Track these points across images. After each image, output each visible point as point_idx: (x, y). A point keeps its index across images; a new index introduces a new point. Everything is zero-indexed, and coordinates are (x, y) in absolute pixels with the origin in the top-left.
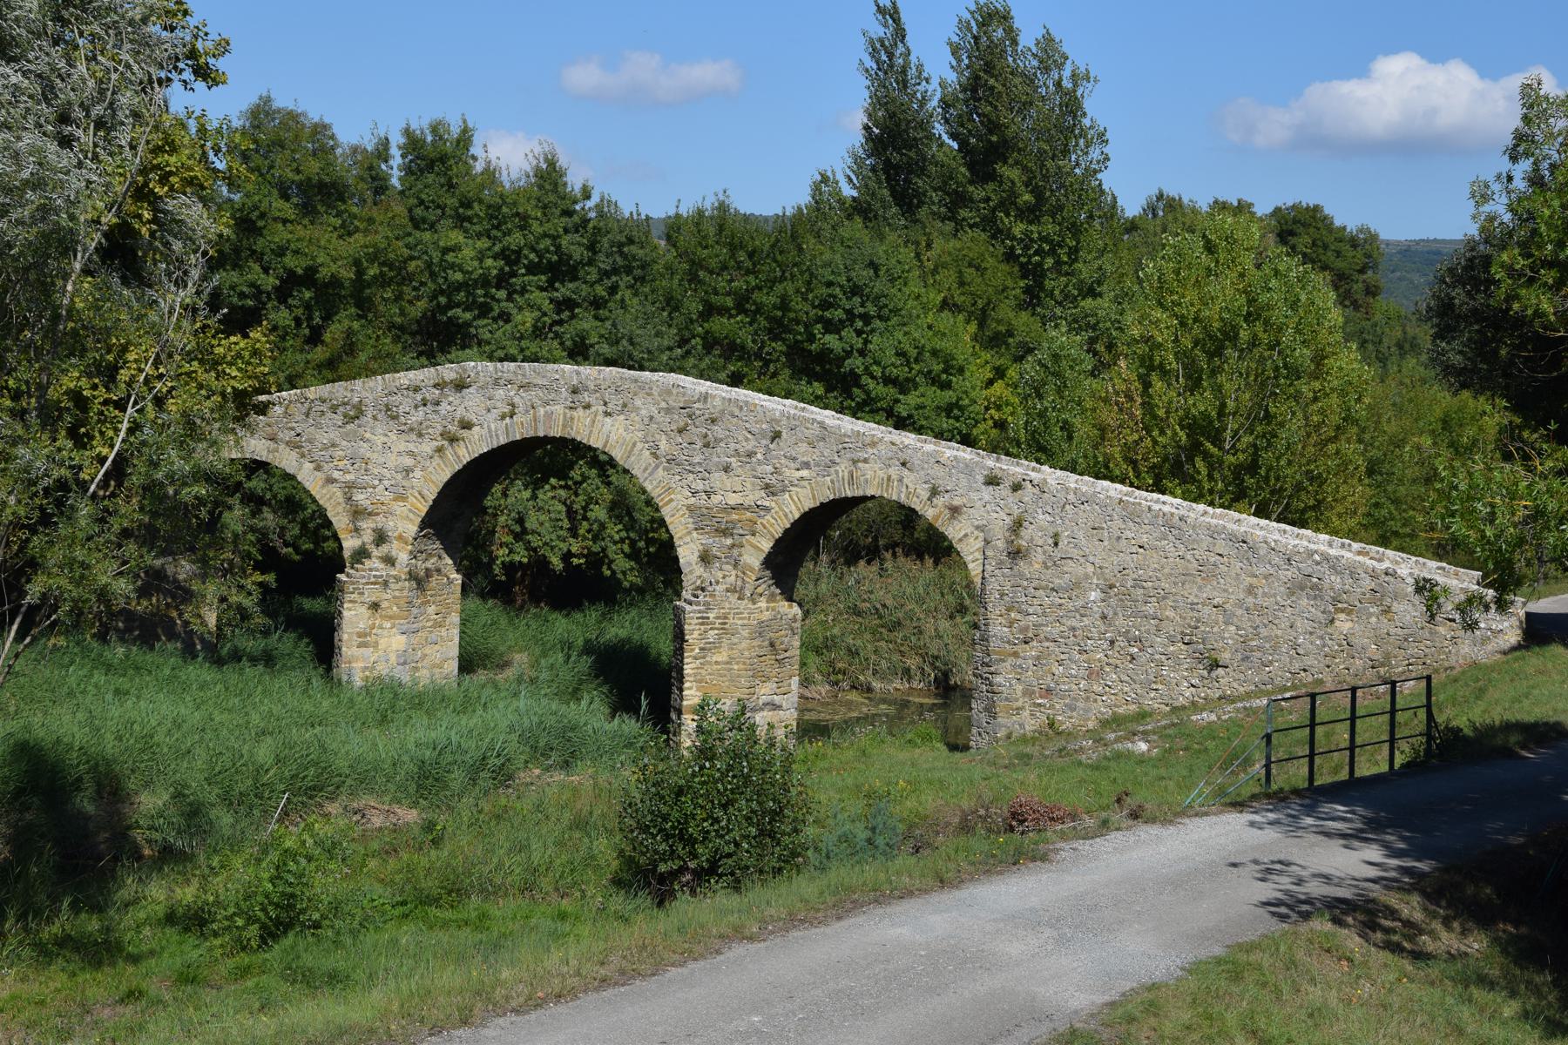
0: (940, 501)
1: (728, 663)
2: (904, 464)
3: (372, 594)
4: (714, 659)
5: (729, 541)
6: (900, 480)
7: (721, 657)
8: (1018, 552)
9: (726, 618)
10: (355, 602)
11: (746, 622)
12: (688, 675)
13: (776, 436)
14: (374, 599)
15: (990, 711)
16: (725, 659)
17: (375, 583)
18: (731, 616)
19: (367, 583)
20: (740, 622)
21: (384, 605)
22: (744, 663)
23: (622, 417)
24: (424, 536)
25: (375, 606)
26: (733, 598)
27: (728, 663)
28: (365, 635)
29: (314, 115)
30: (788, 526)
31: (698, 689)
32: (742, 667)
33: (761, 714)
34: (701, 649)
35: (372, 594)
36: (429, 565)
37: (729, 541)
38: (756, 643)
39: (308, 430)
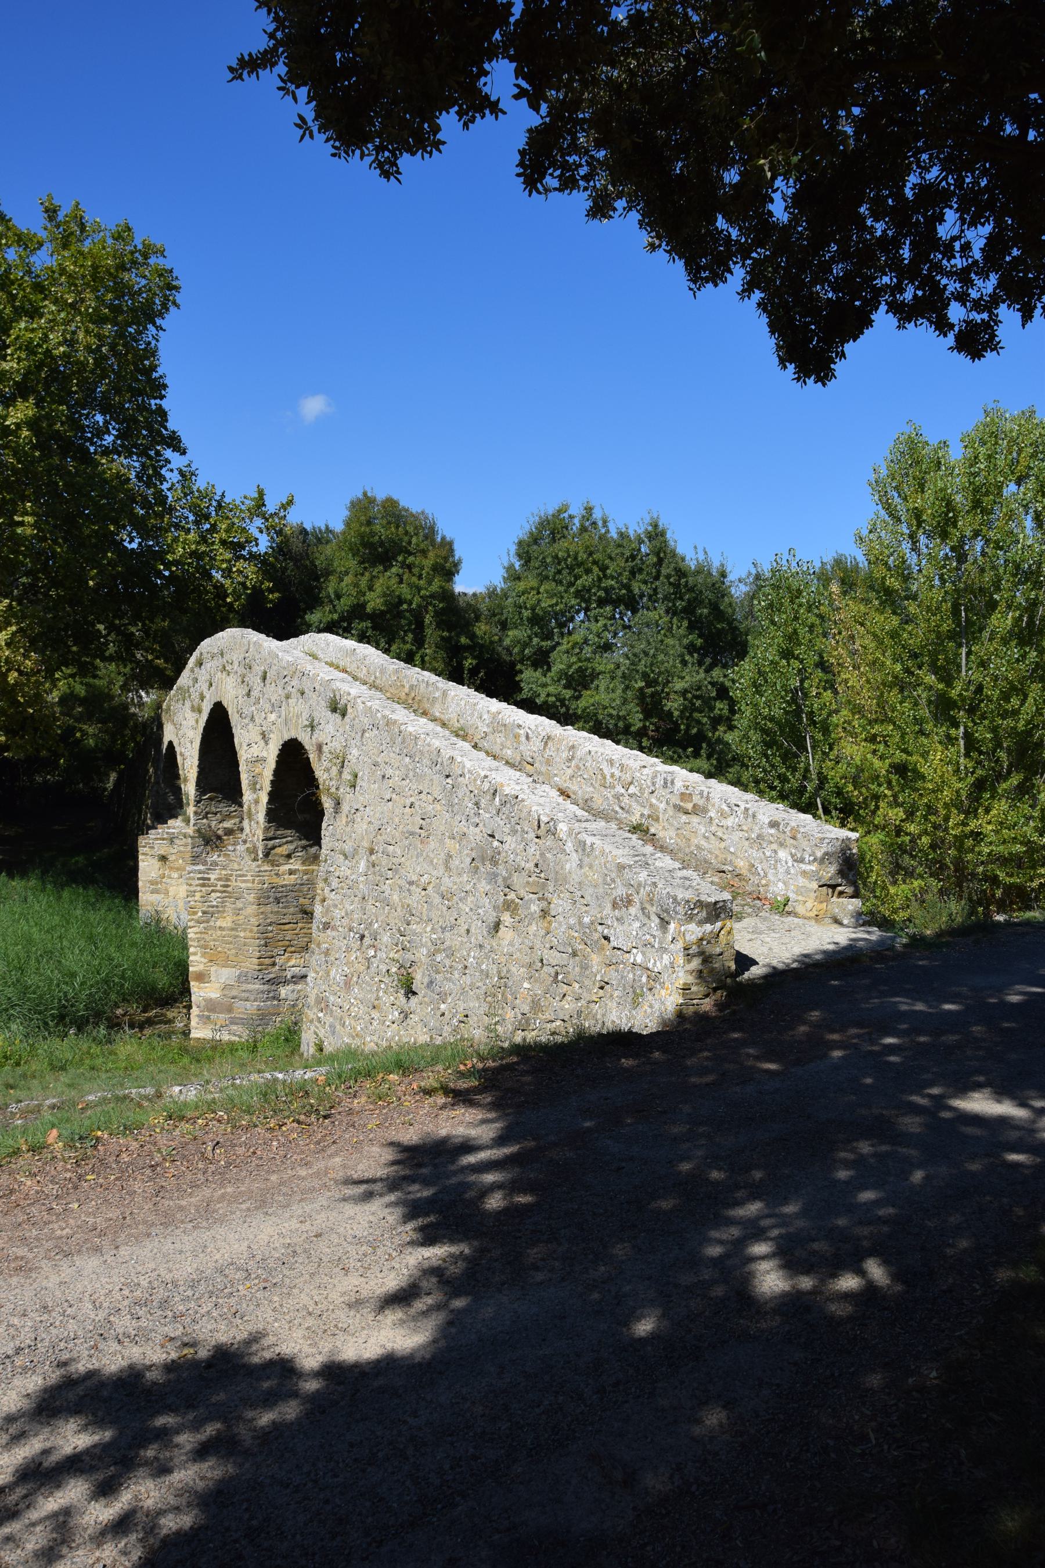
1: (232, 929)
3: (161, 848)
4: (218, 924)
7: (226, 922)
9: (228, 880)
10: (146, 854)
11: (250, 885)
12: (193, 940)
14: (162, 852)
16: (230, 925)
17: (163, 839)
18: (233, 878)
19: (157, 839)
20: (243, 885)
21: (172, 858)
22: (251, 931)
24: (211, 799)
25: (163, 858)
26: (248, 859)
27: (232, 929)
28: (157, 883)
29: (380, 495)
30: (271, 778)
31: (204, 955)
32: (249, 934)
33: (290, 987)
34: (204, 913)
35: (161, 848)
36: (227, 824)
38: (268, 908)
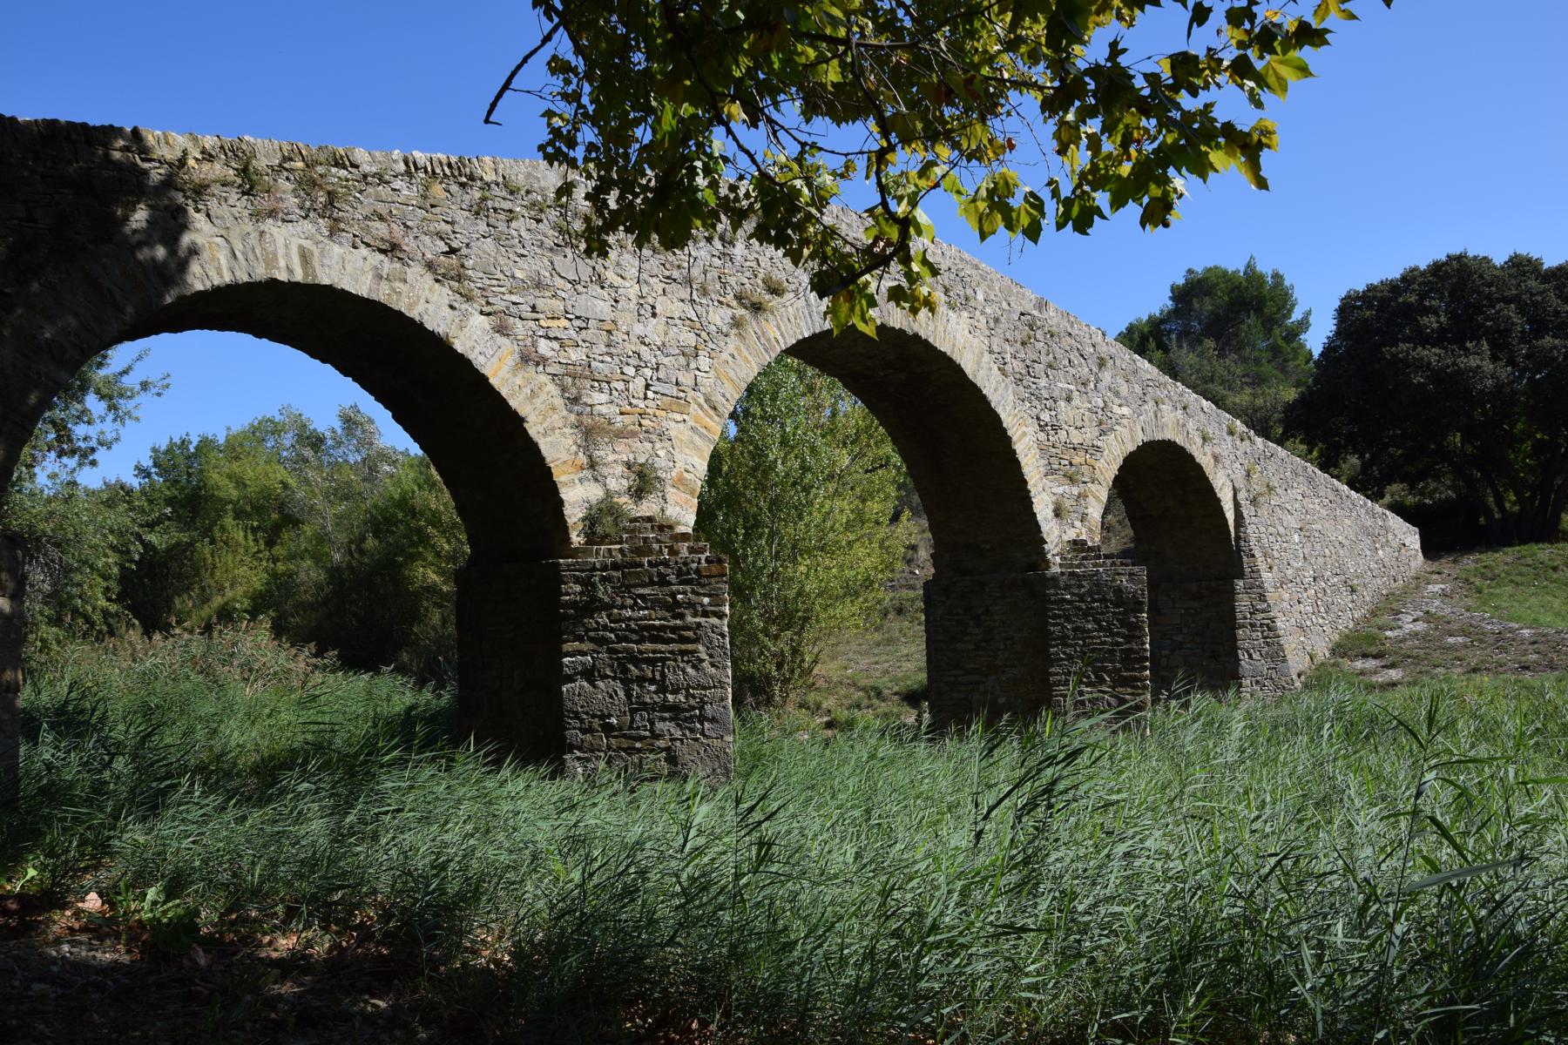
0: (1208, 449)
2: (1185, 408)
5: (1075, 491)
6: (1184, 425)
8: (1255, 499)
13: (1102, 364)
15: (1276, 655)
23: (965, 314)
37: (1075, 491)
39: (482, 252)
